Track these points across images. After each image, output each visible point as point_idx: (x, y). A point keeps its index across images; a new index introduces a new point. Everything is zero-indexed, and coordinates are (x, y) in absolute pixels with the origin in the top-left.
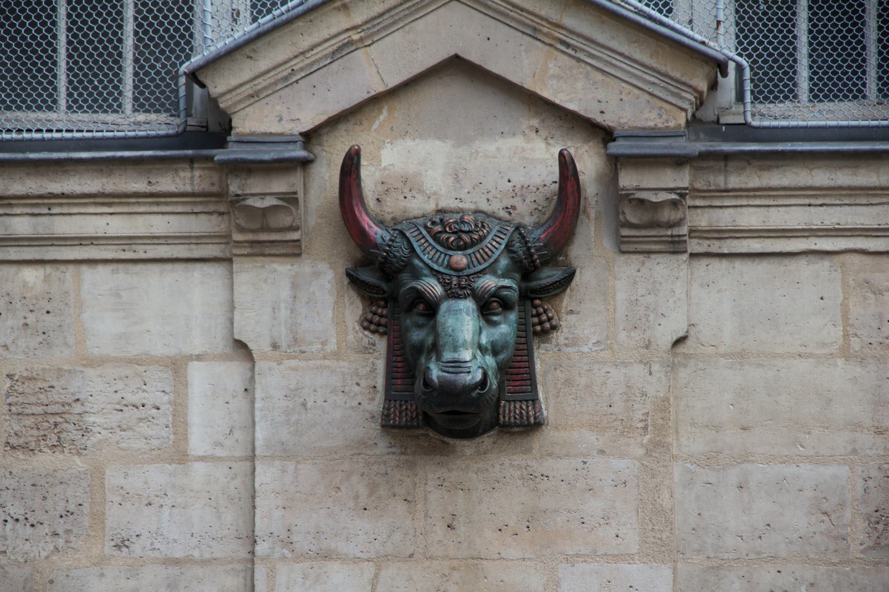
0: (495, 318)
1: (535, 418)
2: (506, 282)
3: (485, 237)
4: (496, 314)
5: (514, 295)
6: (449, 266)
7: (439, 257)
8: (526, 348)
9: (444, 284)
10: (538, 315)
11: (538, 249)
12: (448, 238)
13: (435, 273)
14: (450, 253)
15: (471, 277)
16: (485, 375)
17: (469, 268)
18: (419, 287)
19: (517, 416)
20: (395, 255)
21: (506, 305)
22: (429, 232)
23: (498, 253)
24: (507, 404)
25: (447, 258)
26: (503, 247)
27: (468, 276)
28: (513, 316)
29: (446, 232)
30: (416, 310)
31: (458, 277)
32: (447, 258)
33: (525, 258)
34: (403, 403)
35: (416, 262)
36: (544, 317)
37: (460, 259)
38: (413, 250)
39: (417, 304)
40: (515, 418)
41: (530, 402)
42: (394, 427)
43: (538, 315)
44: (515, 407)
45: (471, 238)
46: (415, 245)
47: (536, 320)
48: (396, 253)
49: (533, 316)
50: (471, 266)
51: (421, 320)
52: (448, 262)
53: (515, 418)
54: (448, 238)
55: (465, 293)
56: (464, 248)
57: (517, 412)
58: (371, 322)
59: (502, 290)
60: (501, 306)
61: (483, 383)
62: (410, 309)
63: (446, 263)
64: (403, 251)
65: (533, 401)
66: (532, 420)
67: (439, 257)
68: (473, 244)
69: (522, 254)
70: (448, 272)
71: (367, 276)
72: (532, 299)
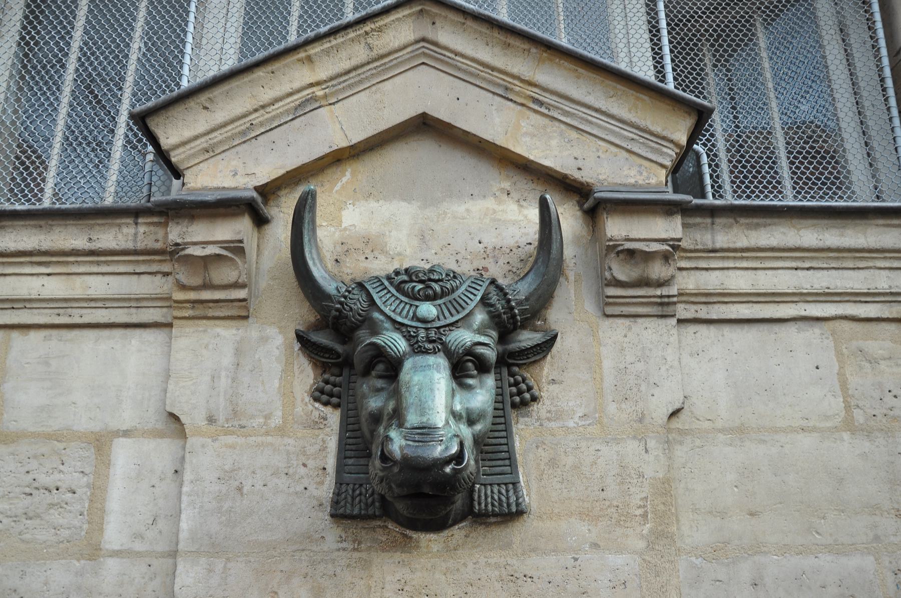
0: (470, 381)
1: (518, 504)
2: (483, 339)
3: (457, 288)
4: (472, 377)
5: (490, 354)
6: (415, 318)
7: (404, 308)
8: (503, 422)
9: (408, 338)
10: (516, 384)
11: (519, 303)
12: (414, 287)
13: (399, 326)
14: (417, 303)
15: (442, 330)
16: (461, 444)
17: (439, 320)
18: (379, 341)
19: (495, 503)
20: (351, 308)
21: (483, 367)
22: (391, 283)
23: (472, 305)
24: (483, 487)
27: (438, 328)
28: (490, 381)
29: (411, 281)
30: (373, 373)
31: (427, 329)
33: (504, 313)
34: (357, 486)
35: (376, 315)
37: (428, 309)
38: (372, 302)
39: (376, 364)
40: (493, 505)
41: (511, 486)
42: (344, 517)
43: (516, 384)
44: (492, 492)
45: (442, 287)
46: (375, 297)
47: (514, 389)
49: (510, 386)
50: (441, 317)
51: (380, 383)
52: (415, 313)
53: (493, 505)
54: (414, 287)
55: (434, 348)
57: (496, 497)
58: (322, 392)
59: (479, 347)
61: (458, 457)
62: (366, 372)
63: (411, 314)
64: (360, 303)
65: (514, 484)
66: (514, 509)
67: (404, 308)
68: (443, 294)
69: (501, 308)
70: (414, 324)
71: (322, 339)
72: (509, 366)
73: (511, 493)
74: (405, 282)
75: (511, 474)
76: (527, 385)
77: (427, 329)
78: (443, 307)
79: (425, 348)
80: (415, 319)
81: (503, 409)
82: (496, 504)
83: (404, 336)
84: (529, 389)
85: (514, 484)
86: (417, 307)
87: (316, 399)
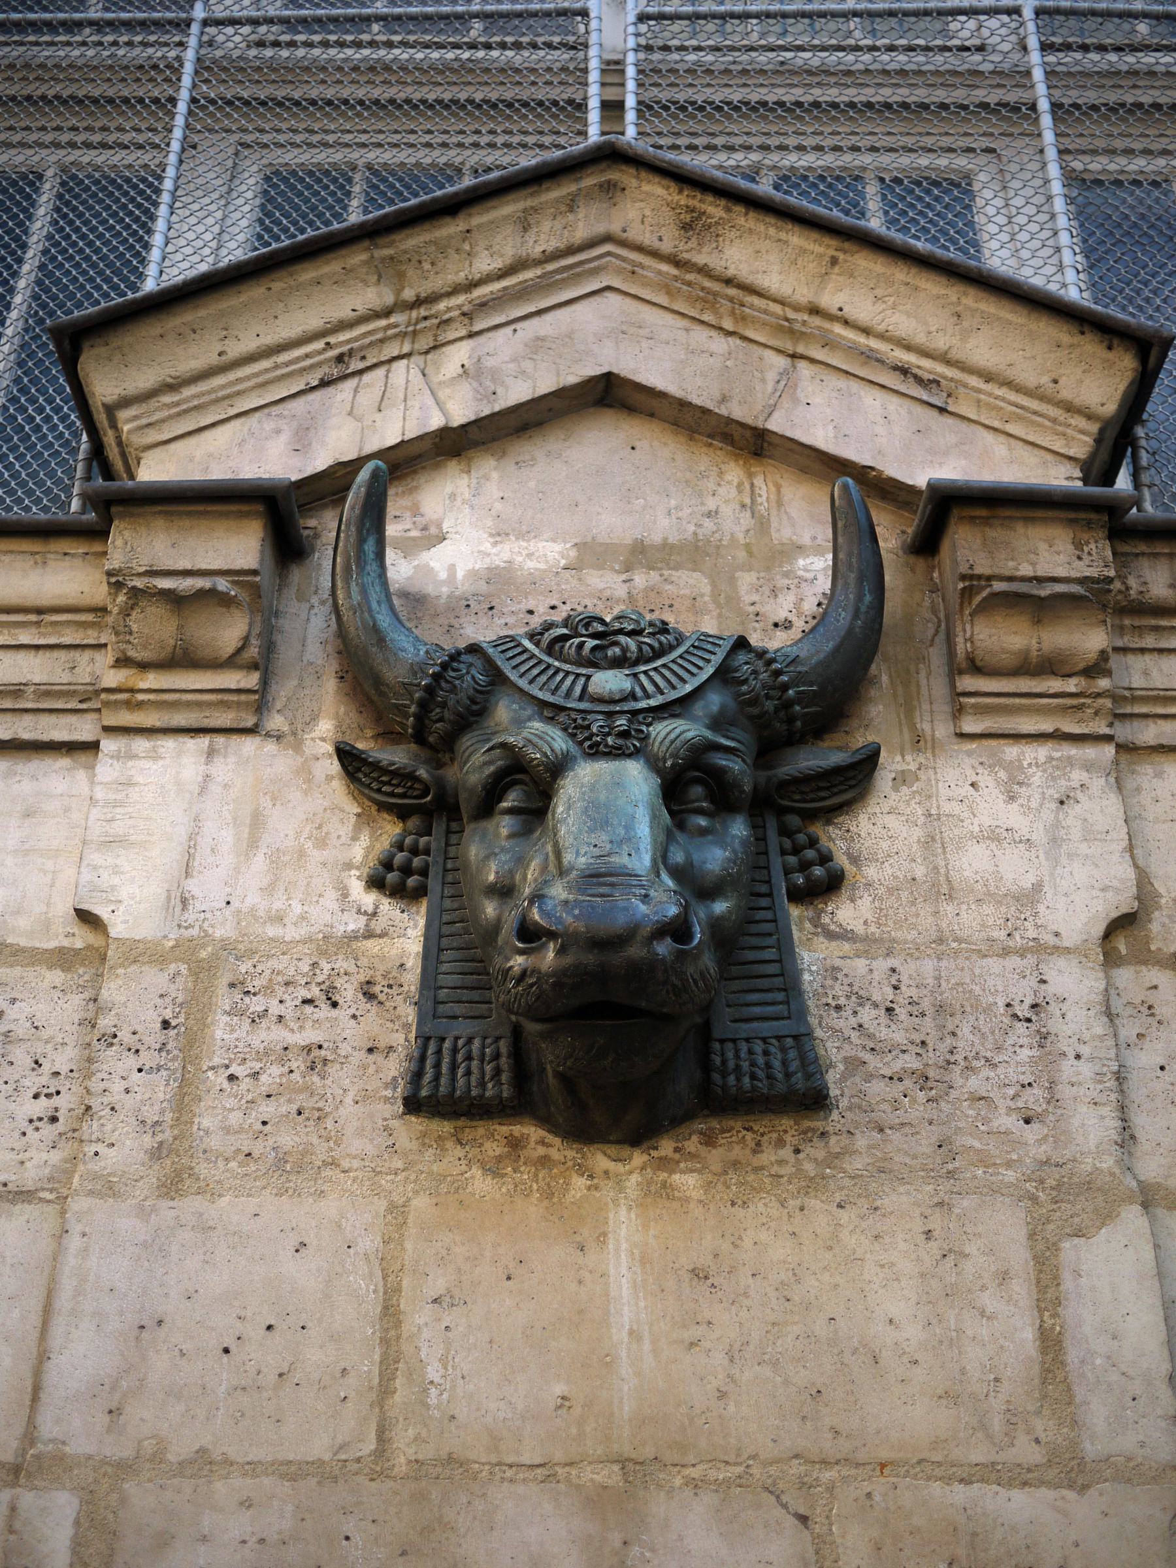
3: (672, 648)
11: (799, 678)
12: (581, 646)
13: (551, 711)
15: (640, 717)
20: (455, 687)
22: (537, 644)
23: (704, 676)
24: (730, 1045)
25: (582, 680)
26: (710, 670)
28: (739, 828)
32: (582, 680)
36: (810, 854)
37: (609, 681)
40: (753, 1077)
41: (789, 1042)
43: (796, 851)
44: (751, 1052)
47: (792, 860)
48: (457, 682)
49: (783, 852)
53: (753, 1077)
54: (581, 646)
56: (618, 663)
57: (761, 1060)
60: (711, 797)
62: (486, 807)
63: (578, 690)
70: (583, 706)
72: (782, 811)
73: (792, 1054)
74: (564, 638)
75: (789, 1018)
76: (818, 851)
77: (610, 715)
78: (642, 677)
79: (606, 746)
80: (587, 697)
81: (770, 895)
82: (761, 1074)
83: (565, 730)
84: (825, 858)
85: (796, 1037)
86: (589, 677)
87: (375, 883)
